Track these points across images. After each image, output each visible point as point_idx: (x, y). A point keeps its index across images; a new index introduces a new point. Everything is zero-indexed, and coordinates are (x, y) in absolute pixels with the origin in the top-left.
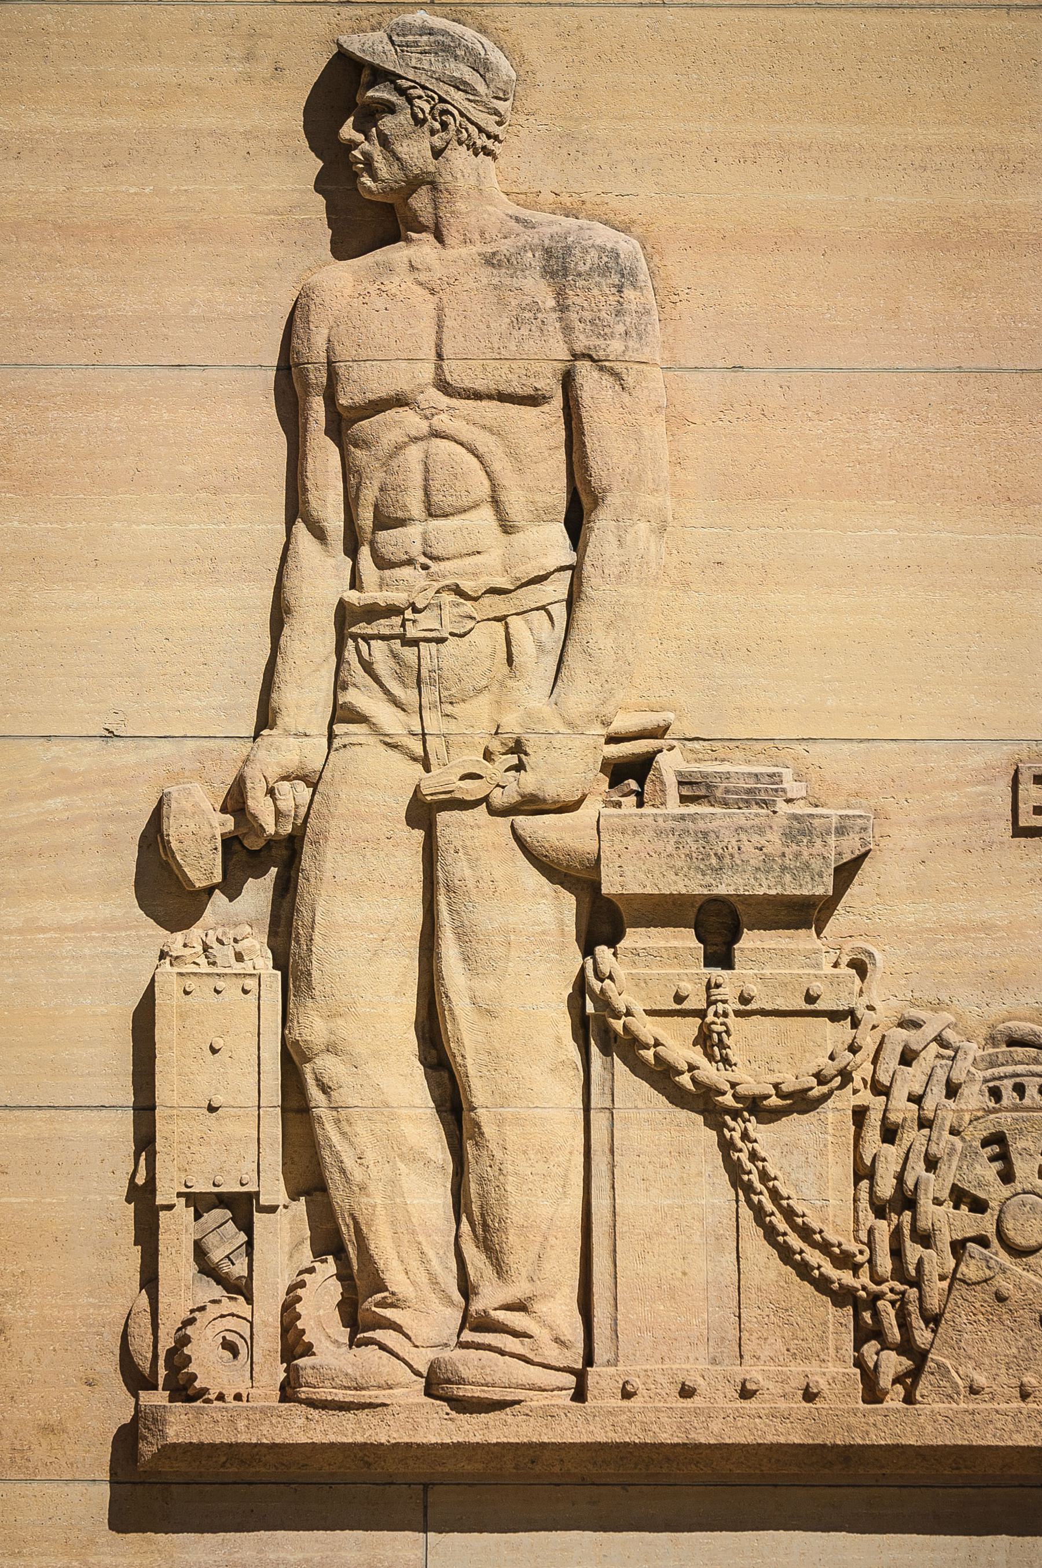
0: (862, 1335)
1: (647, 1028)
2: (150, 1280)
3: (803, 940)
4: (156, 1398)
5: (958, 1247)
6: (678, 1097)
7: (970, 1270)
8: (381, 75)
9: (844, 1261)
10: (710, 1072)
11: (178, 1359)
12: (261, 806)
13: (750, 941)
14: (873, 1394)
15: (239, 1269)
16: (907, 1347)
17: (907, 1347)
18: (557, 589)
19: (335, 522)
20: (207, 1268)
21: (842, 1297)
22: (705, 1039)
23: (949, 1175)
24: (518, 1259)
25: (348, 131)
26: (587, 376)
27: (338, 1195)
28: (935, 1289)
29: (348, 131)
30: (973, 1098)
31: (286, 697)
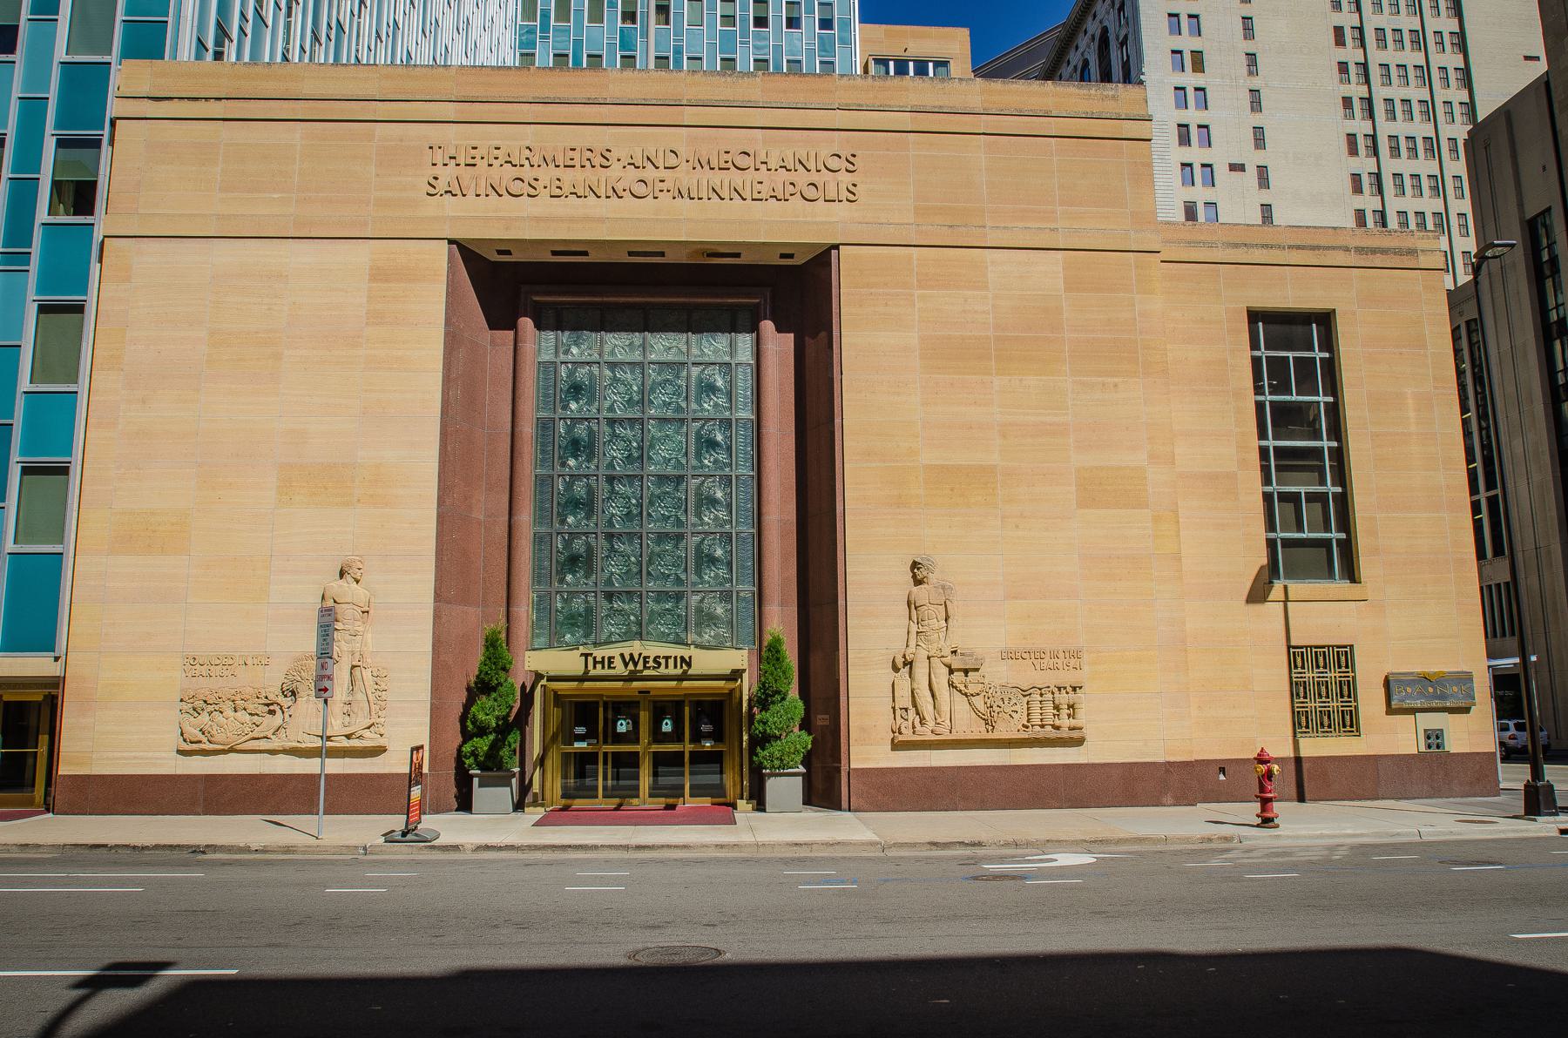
0: (986, 724)
1: (958, 685)
2: (895, 719)
3: (976, 673)
4: (897, 734)
5: (998, 713)
6: (962, 694)
7: (1000, 715)
8: (920, 564)
9: (984, 715)
10: (966, 691)
11: (899, 728)
12: (908, 658)
13: (970, 674)
14: (988, 732)
15: (906, 717)
16: (992, 725)
17: (992, 725)
18: (945, 629)
19: (916, 621)
20: (902, 717)
21: (984, 719)
22: (965, 686)
23: (997, 703)
24: (943, 715)
25: (916, 570)
26: (948, 602)
27: (918, 706)
28: (995, 718)
29: (916, 570)
30: (999, 693)
31: (910, 643)
